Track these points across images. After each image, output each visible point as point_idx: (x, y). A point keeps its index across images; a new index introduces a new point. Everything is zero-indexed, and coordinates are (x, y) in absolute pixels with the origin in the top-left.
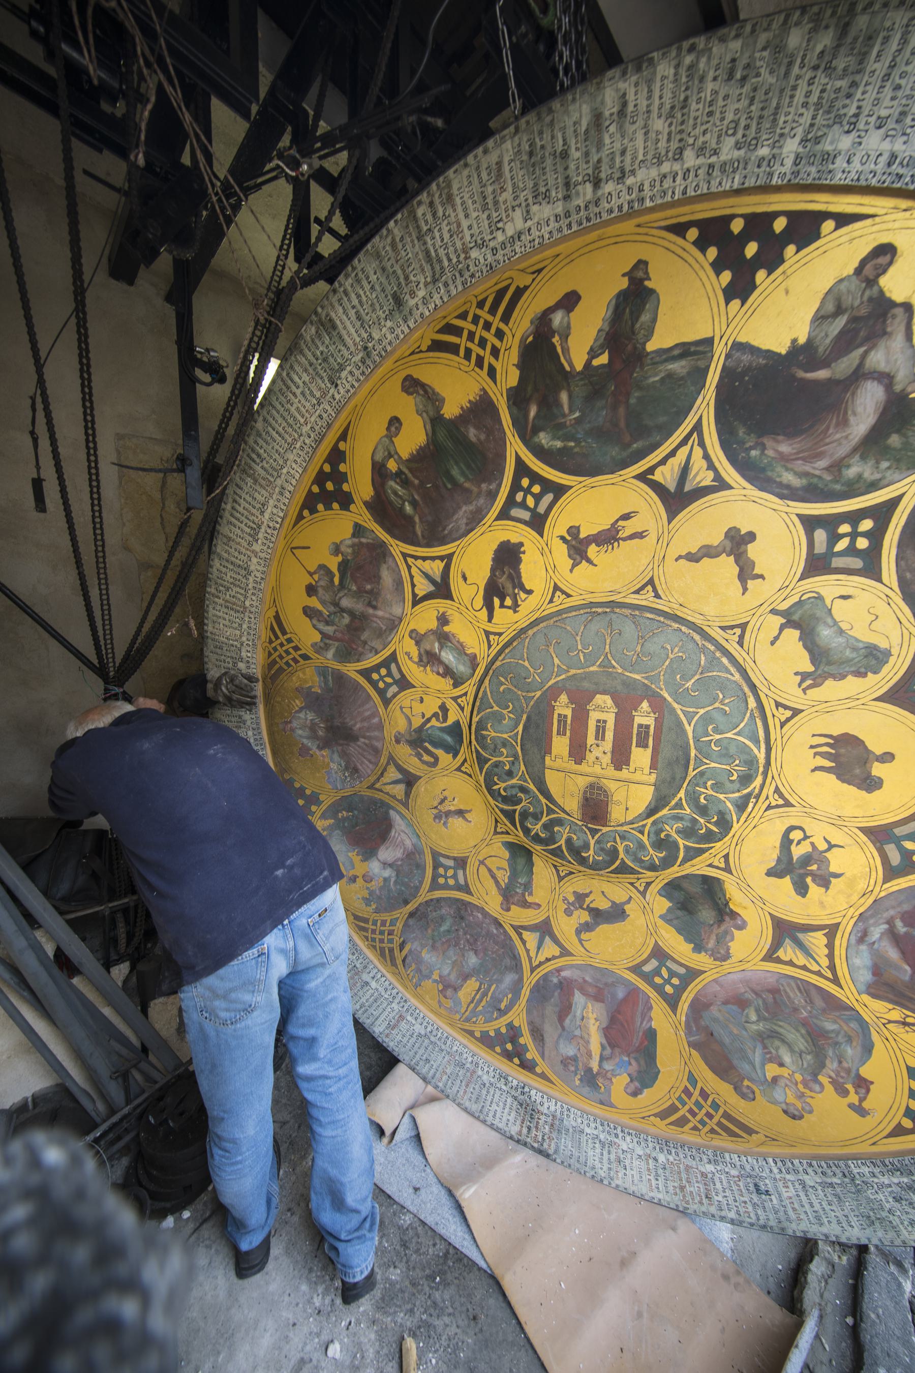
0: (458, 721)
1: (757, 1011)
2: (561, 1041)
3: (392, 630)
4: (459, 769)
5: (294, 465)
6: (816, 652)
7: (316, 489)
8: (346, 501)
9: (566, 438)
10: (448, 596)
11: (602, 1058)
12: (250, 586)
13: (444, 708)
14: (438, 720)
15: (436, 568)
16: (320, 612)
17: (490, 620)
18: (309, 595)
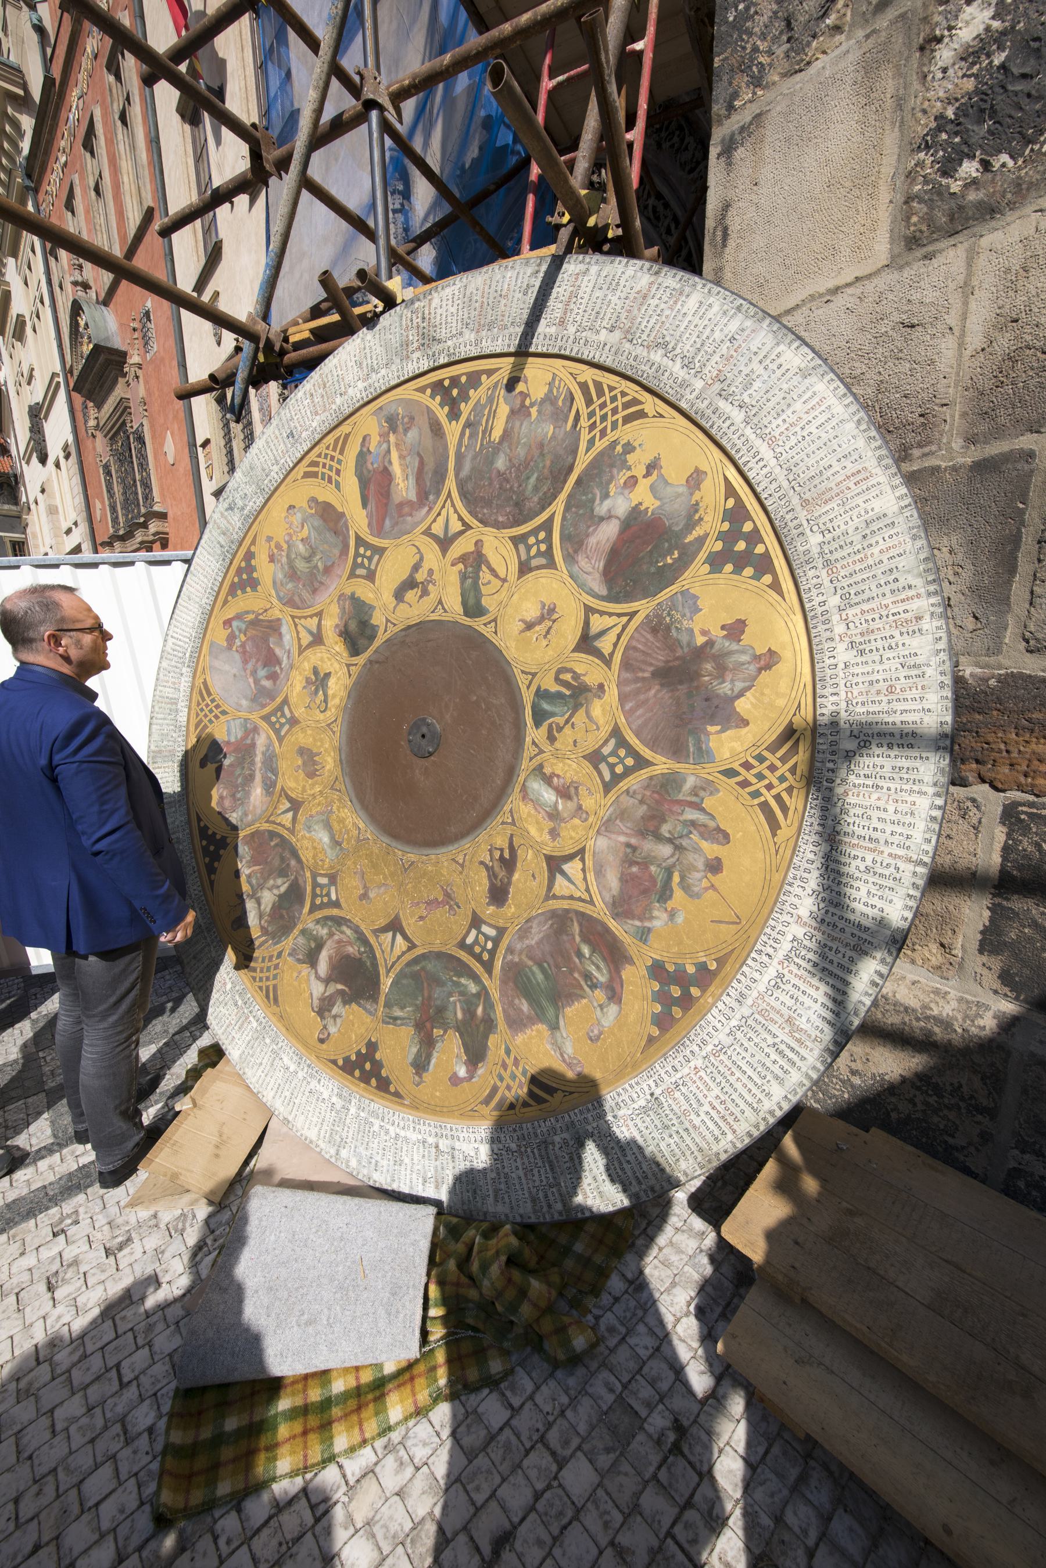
3: (609, 820)
4: (534, 675)
5: (719, 1026)
7: (695, 991)
8: (657, 970)
9: (457, 984)
10: (549, 859)
11: (389, 451)
13: (551, 739)
15: (561, 885)
16: (702, 836)
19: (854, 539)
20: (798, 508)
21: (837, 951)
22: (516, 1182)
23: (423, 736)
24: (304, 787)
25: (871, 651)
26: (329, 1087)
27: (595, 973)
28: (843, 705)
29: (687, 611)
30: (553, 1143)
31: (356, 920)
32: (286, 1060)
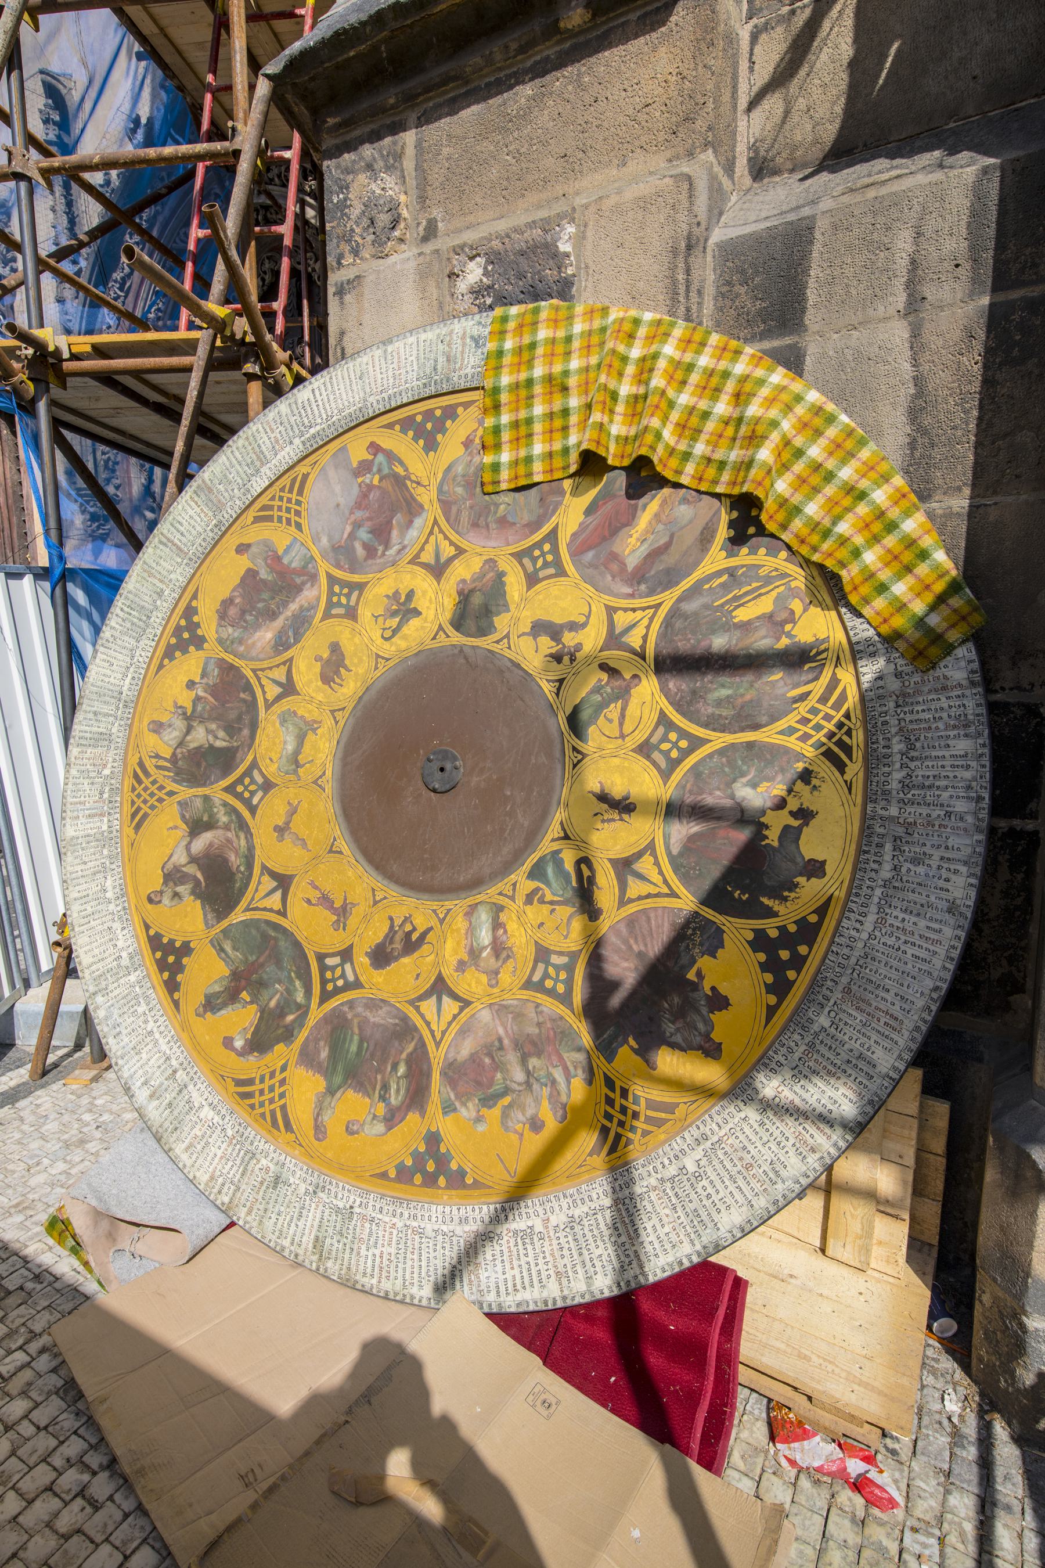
0: (528, 878)
1: (496, 512)
2: (684, 522)
3: (505, 1007)
5: (434, 1219)
6: (301, 739)
7: (442, 1181)
9: (291, 981)
10: (440, 979)
12: (585, 1209)
13: (529, 899)
14: (543, 895)
15: (429, 1007)
16: (550, 1097)
17: (431, 928)
18: (543, 1124)
19: (843, 1054)
20: (840, 988)
22: (211, 1155)
23: (442, 770)
24: (310, 681)
25: (767, 1130)
28: (715, 1139)
29: (707, 944)
30: (258, 1161)
32: (109, 883)
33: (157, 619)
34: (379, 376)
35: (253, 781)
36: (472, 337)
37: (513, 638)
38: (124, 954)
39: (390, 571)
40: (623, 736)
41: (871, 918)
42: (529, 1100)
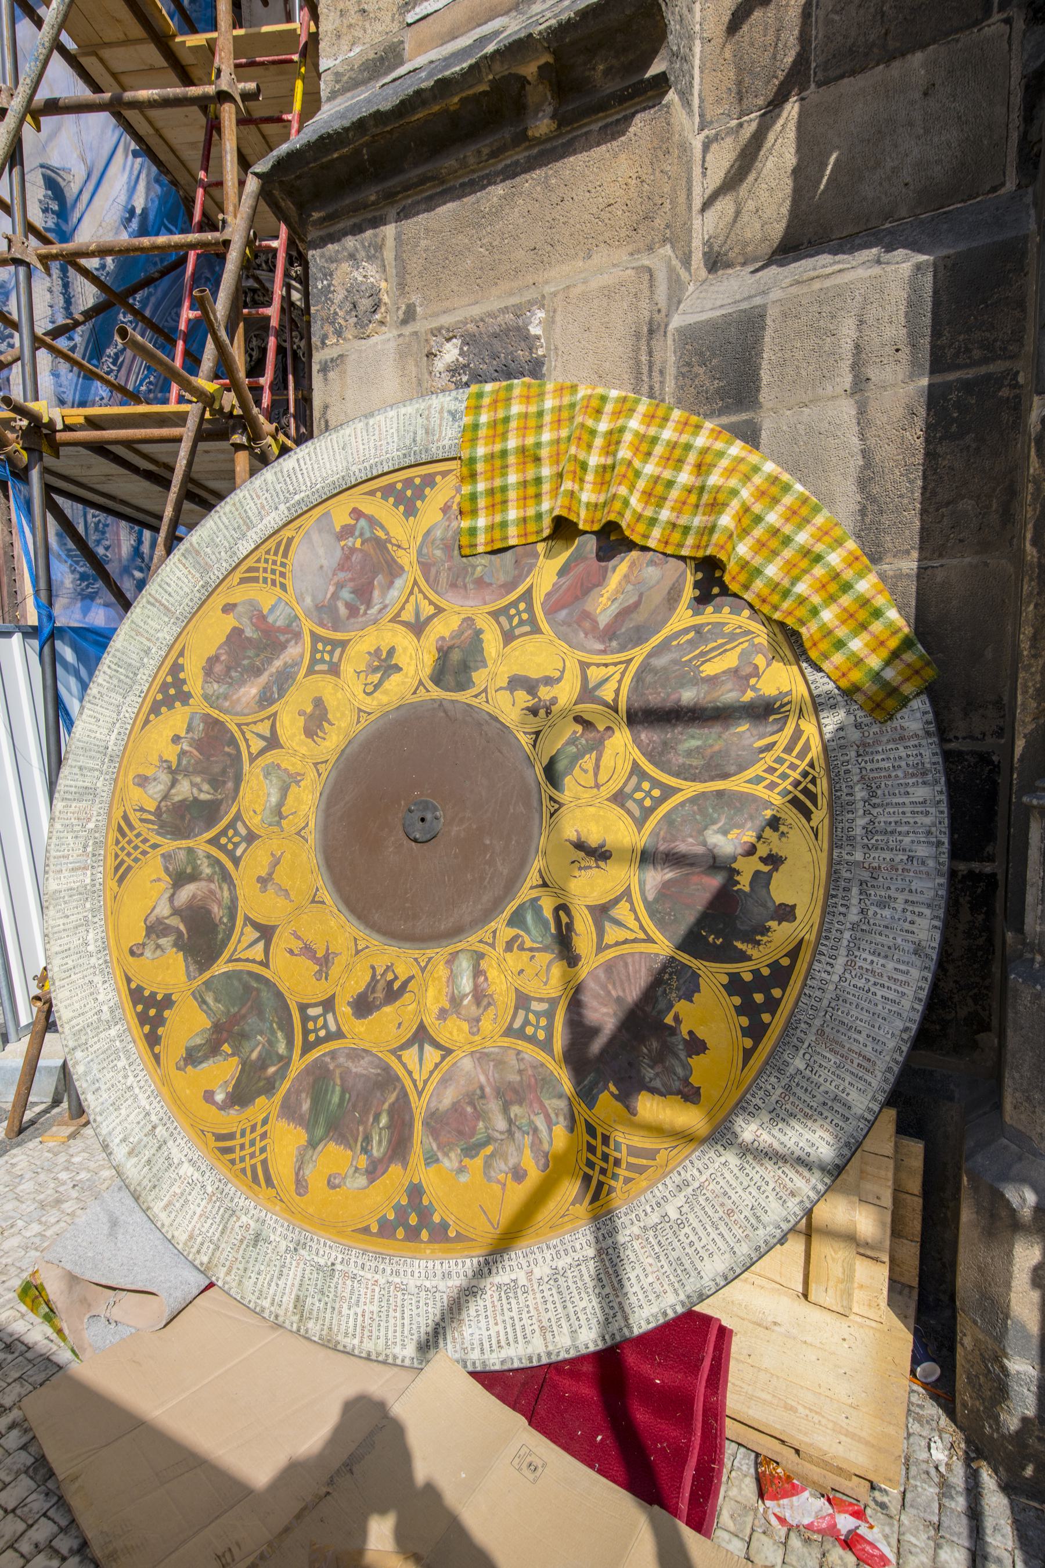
1: (473, 574)
2: (653, 582)
3: (487, 1055)
5: (416, 1275)
6: (284, 791)
7: (425, 1235)
9: (273, 1032)
12: (569, 1260)
13: (509, 947)
15: (410, 1056)
16: (533, 1145)
18: (525, 1173)
20: (814, 1030)
21: (531, 1318)
22: (190, 1213)
23: (423, 820)
24: (294, 735)
26: (108, 995)
27: (375, 1143)
28: (696, 1185)
30: (238, 1218)
31: (239, 892)
32: (91, 936)
33: (144, 676)
34: (361, 447)
35: (236, 833)
36: (449, 412)
37: (491, 692)
38: (105, 1008)
39: (371, 629)
40: (597, 786)
41: (841, 961)
42: (511, 1149)
